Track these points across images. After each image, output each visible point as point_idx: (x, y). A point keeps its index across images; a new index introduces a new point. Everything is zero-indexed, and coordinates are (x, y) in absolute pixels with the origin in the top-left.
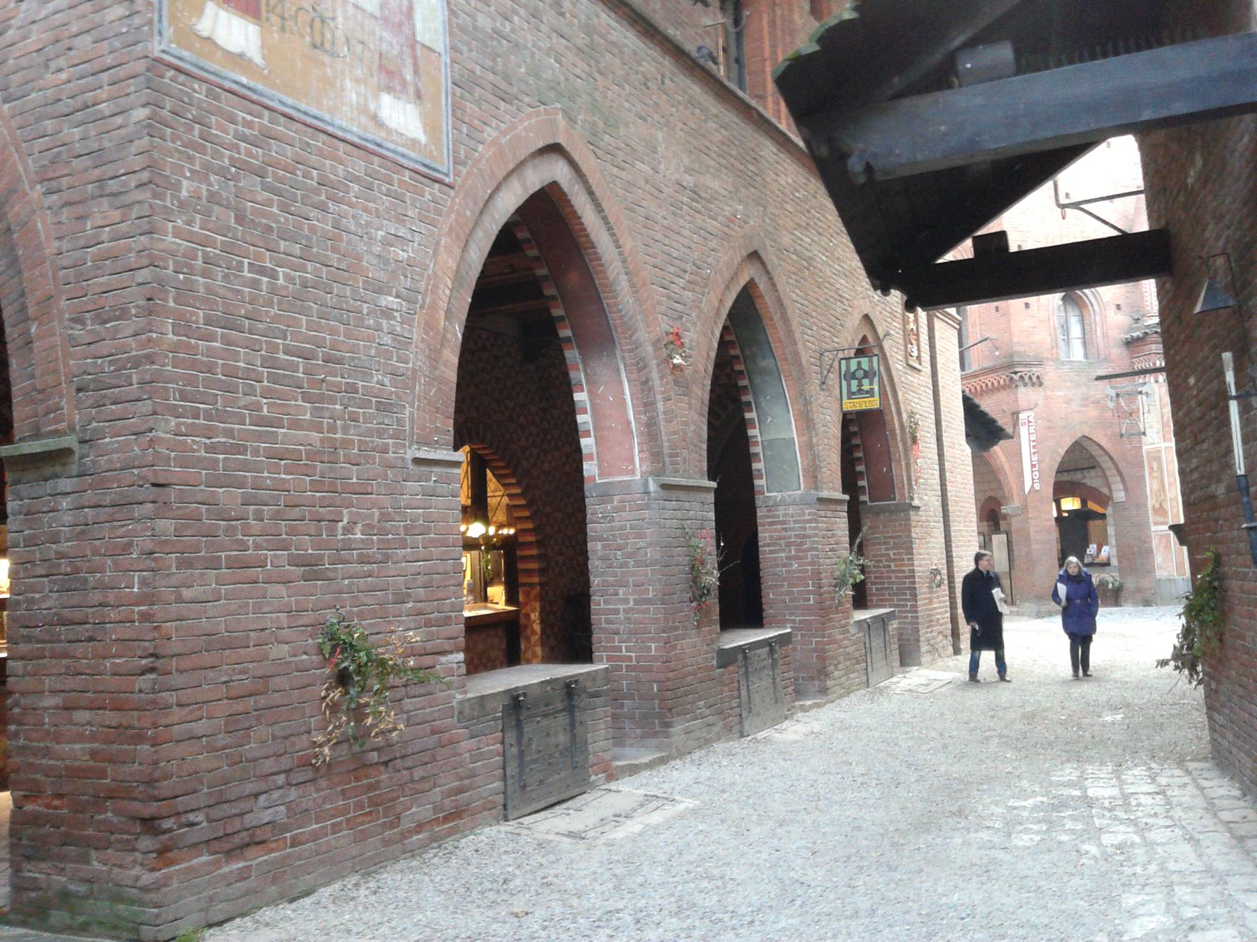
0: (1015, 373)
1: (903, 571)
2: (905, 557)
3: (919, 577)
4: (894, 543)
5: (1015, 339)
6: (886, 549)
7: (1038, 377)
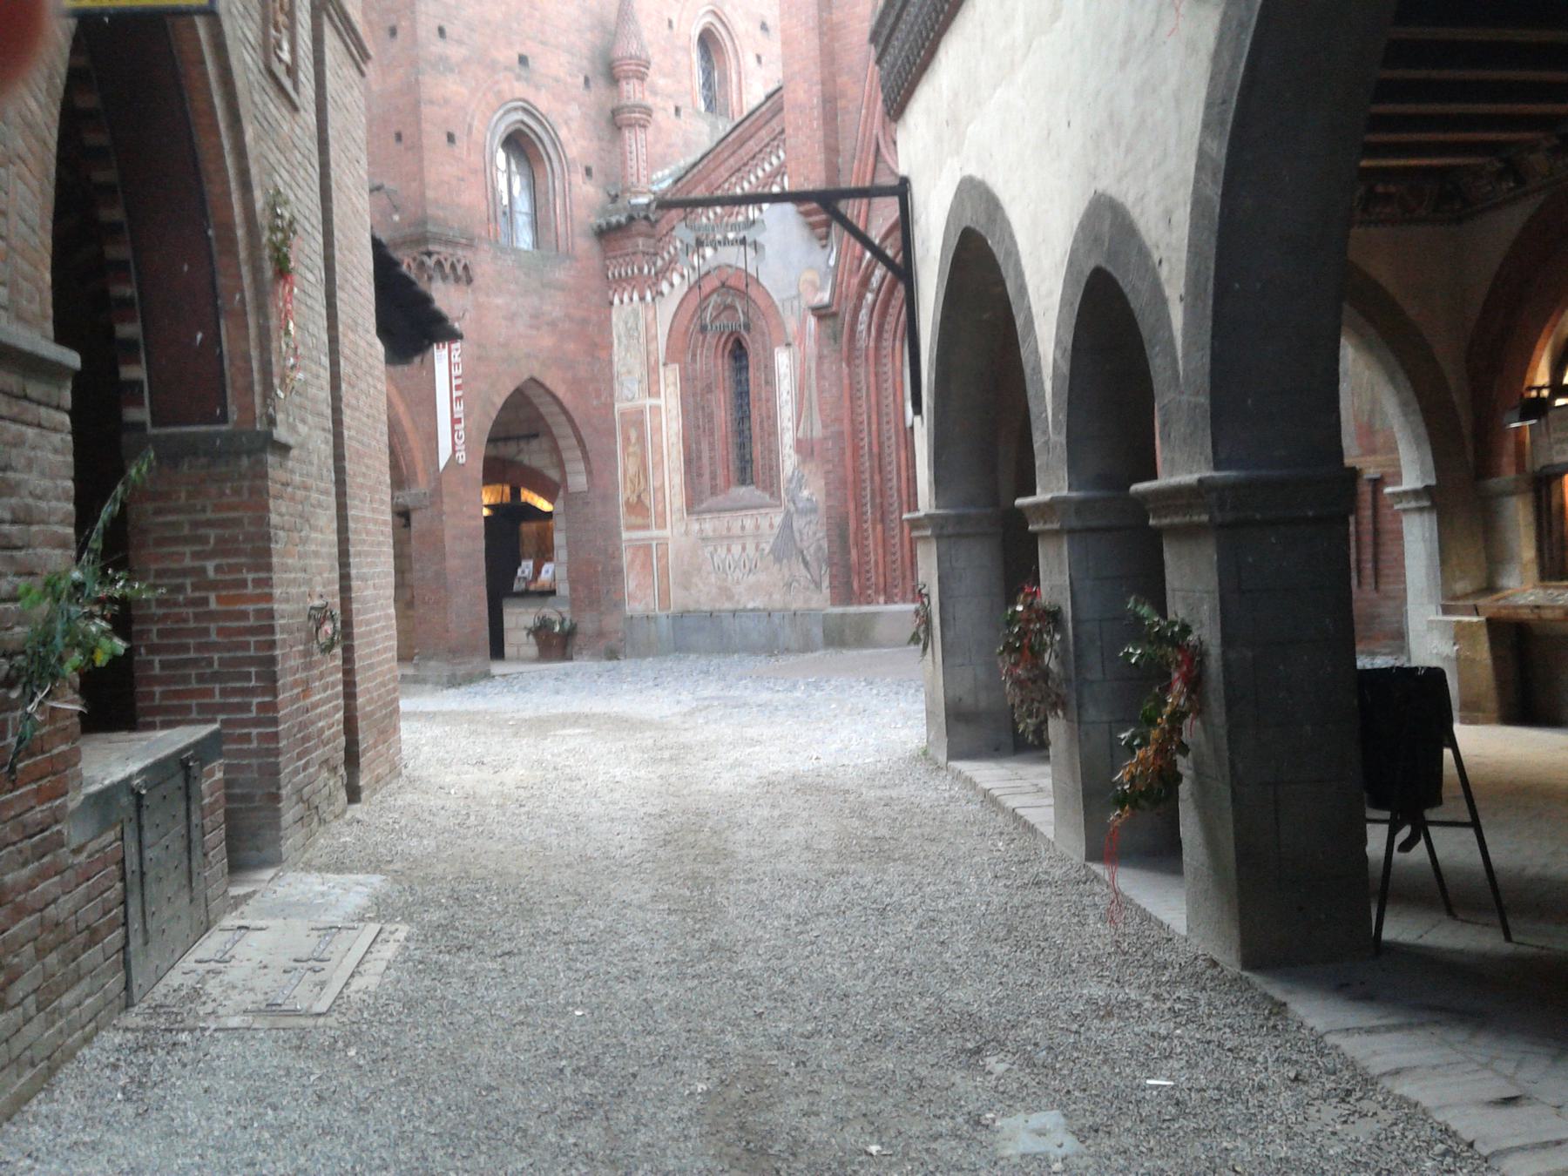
0: (429, 254)
1: (244, 615)
2: (250, 576)
3: (284, 629)
4: (220, 540)
5: (430, 194)
6: (195, 555)
7: (466, 267)
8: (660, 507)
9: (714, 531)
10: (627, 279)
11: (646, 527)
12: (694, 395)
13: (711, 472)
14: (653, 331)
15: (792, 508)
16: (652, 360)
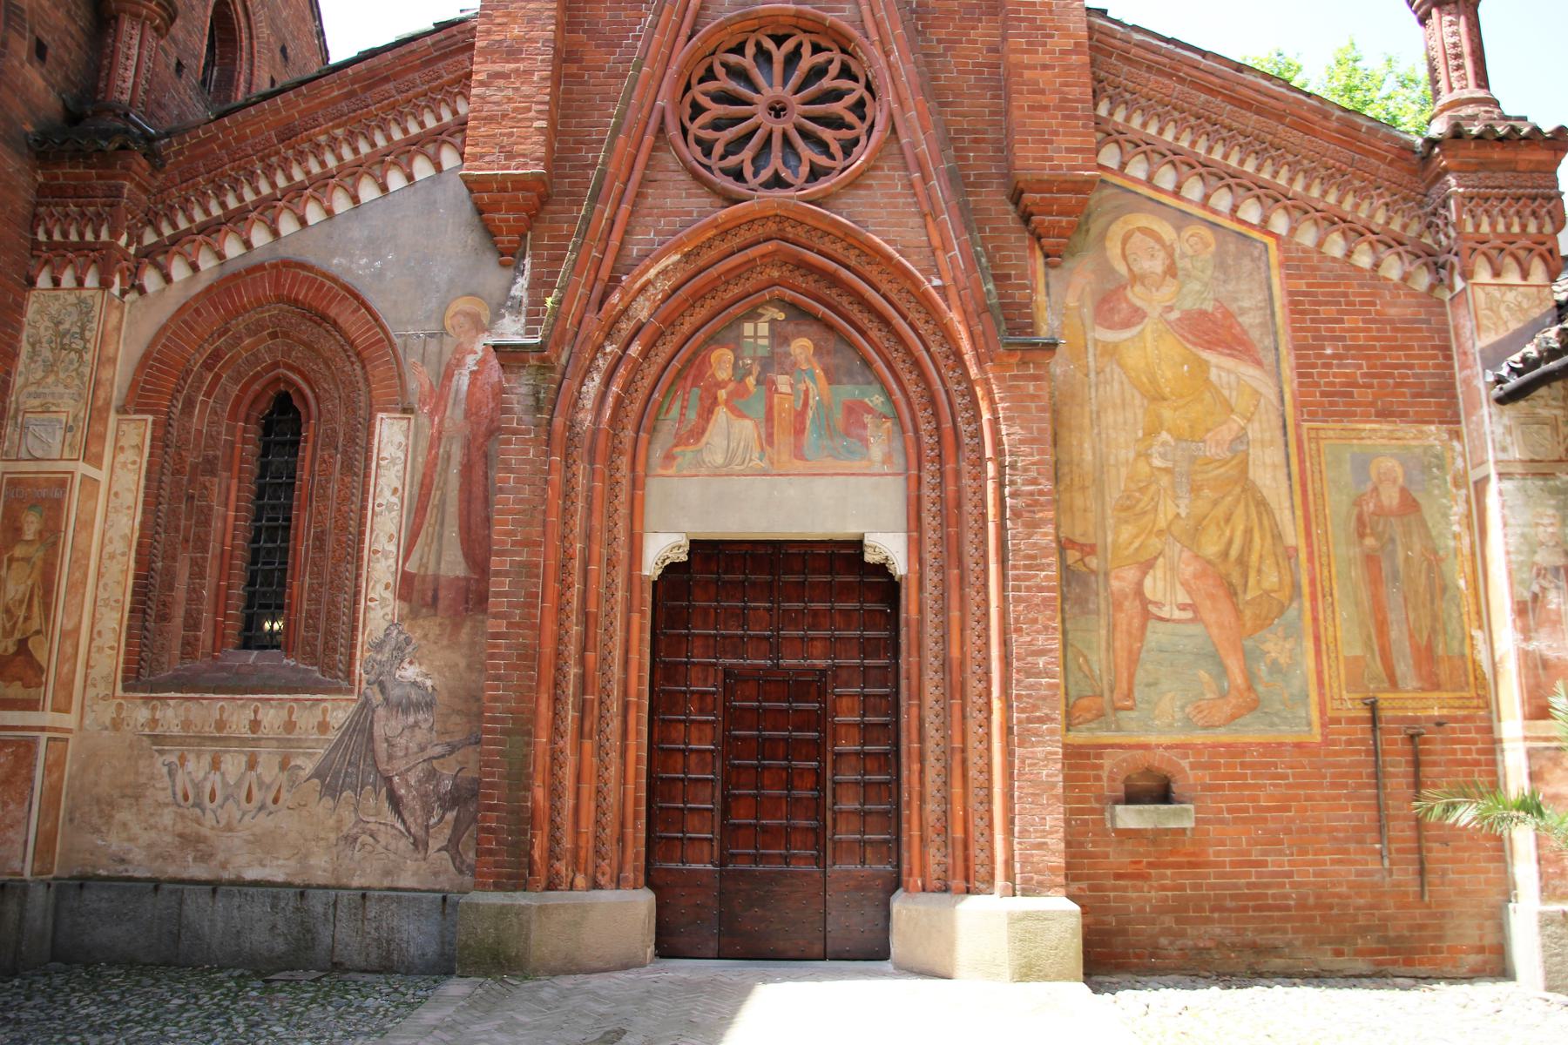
8: (66, 668)
9: (186, 724)
10: (81, 247)
11: (31, 705)
12: (176, 472)
13: (188, 613)
14: (110, 350)
15: (377, 698)
16: (101, 394)
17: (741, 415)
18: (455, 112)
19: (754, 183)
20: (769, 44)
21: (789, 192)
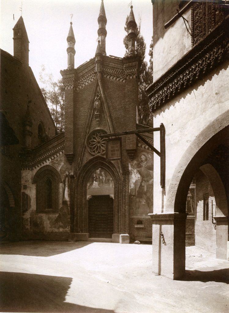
17: (96, 181)
18: (64, 145)
19: (96, 153)
20: (98, 134)
21: (100, 154)
